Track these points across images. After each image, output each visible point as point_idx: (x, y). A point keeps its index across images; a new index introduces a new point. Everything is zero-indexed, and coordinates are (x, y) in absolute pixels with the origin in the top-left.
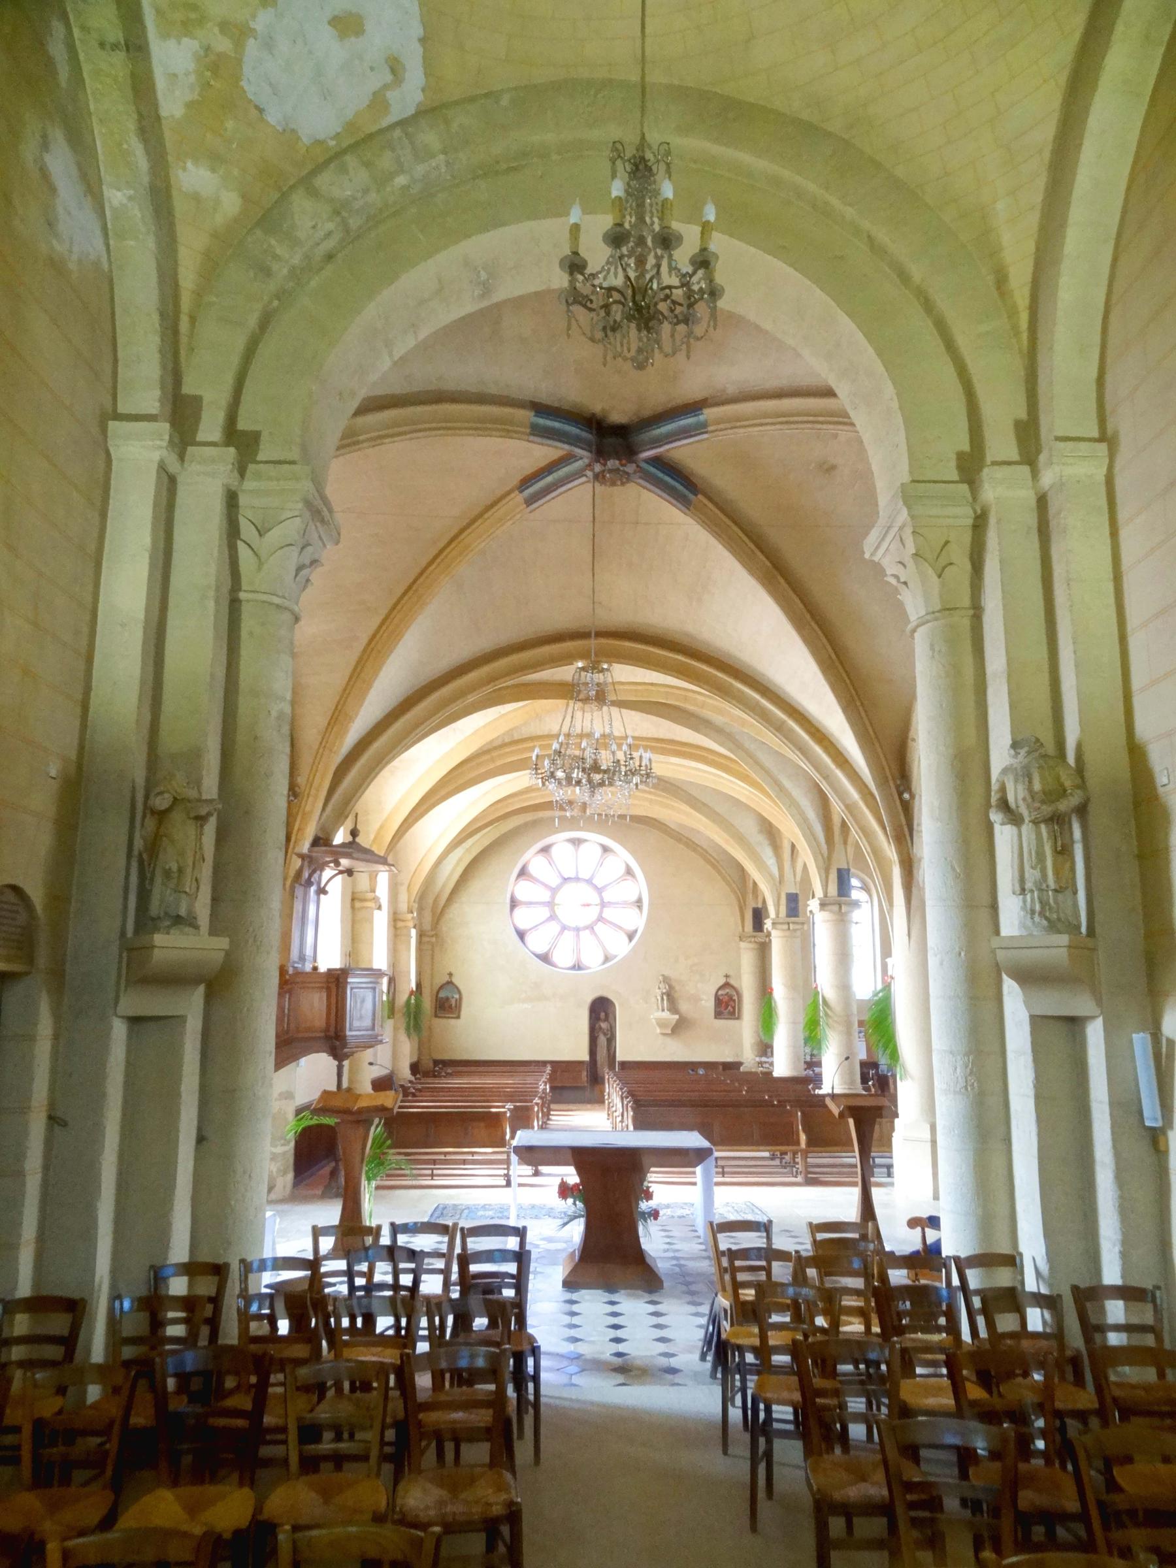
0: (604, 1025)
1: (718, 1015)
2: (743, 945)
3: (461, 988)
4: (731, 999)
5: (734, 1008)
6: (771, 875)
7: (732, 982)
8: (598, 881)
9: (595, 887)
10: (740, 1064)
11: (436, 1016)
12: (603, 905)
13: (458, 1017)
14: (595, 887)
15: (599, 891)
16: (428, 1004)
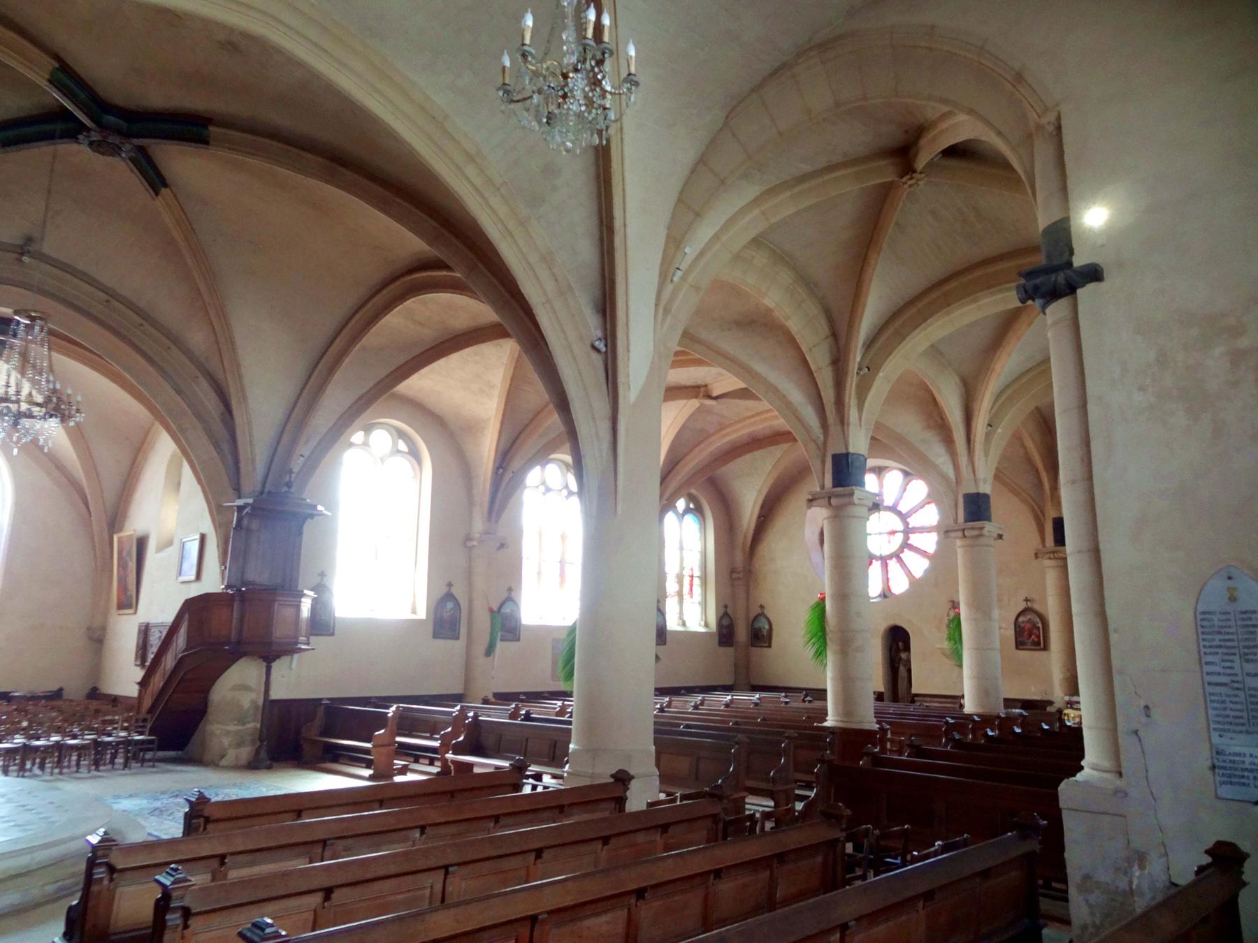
0: (903, 655)
1: (1019, 645)
2: (1047, 563)
3: (771, 619)
4: (1035, 626)
5: (1038, 637)
6: (944, 477)
7: (1037, 607)
8: (903, 508)
9: (899, 513)
10: (1050, 703)
11: (753, 645)
12: (908, 531)
13: (770, 646)
14: (899, 513)
15: (904, 517)
16: (742, 634)
